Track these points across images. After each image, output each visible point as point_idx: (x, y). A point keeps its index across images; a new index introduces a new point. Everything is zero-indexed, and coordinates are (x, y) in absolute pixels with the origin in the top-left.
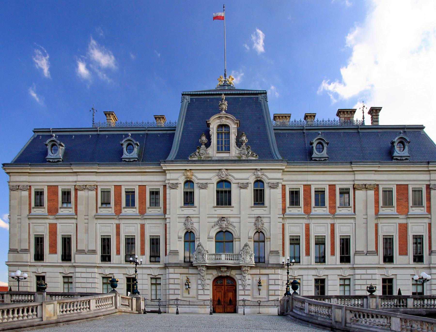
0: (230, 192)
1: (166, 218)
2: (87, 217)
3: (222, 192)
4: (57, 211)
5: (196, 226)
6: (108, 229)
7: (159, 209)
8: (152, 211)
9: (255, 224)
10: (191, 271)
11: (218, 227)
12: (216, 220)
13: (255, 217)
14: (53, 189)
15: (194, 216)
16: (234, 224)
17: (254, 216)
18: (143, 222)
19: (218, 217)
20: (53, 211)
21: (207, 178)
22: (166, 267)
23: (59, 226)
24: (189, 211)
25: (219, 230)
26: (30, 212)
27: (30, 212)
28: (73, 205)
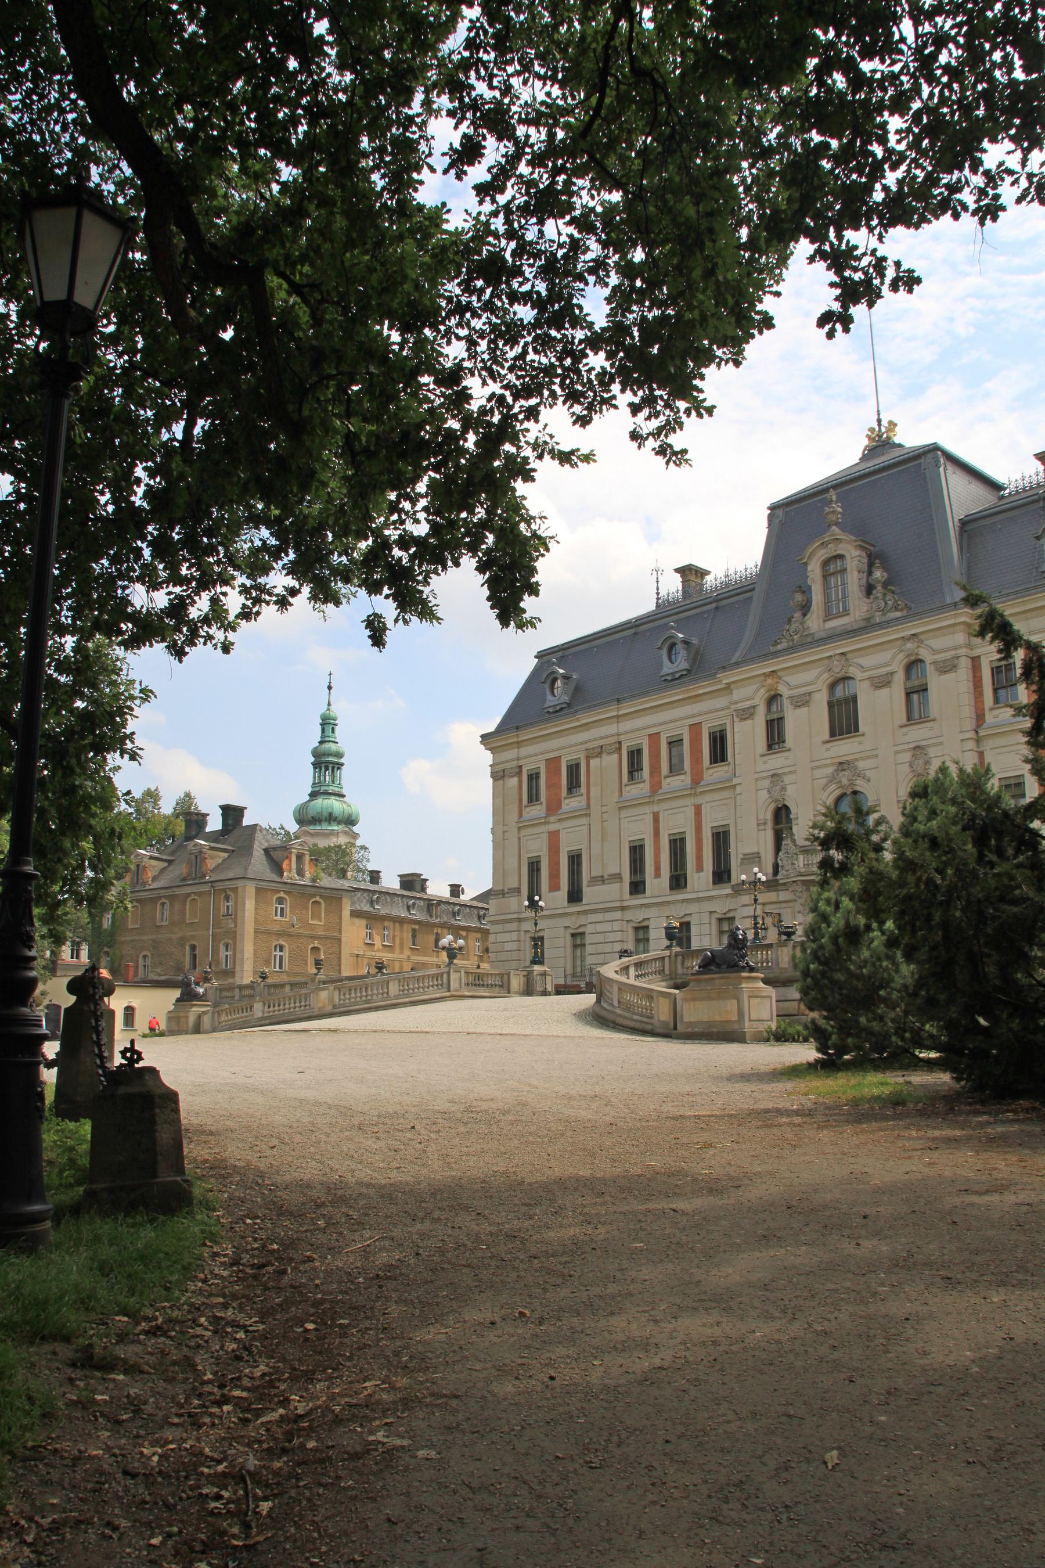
0: (854, 699)
1: (734, 786)
2: (604, 809)
3: (839, 702)
4: (560, 806)
5: (791, 791)
6: (639, 828)
7: (726, 768)
8: (714, 774)
9: (911, 766)
10: (783, 896)
11: (834, 787)
12: (830, 770)
13: (909, 750)
14: (553, 763)
15: (787, 770)
16: (868, 773)
17: (906, 747)
18: (699, 800)
19: (832, 764)
20: (554, 807)
21: (805, 677)
22: (739, 889)
23: (563, 836)
24: (776, 762)
25: (838, 793)
26: (521, 815)
27: (521, 815)
28: (583, 789)
